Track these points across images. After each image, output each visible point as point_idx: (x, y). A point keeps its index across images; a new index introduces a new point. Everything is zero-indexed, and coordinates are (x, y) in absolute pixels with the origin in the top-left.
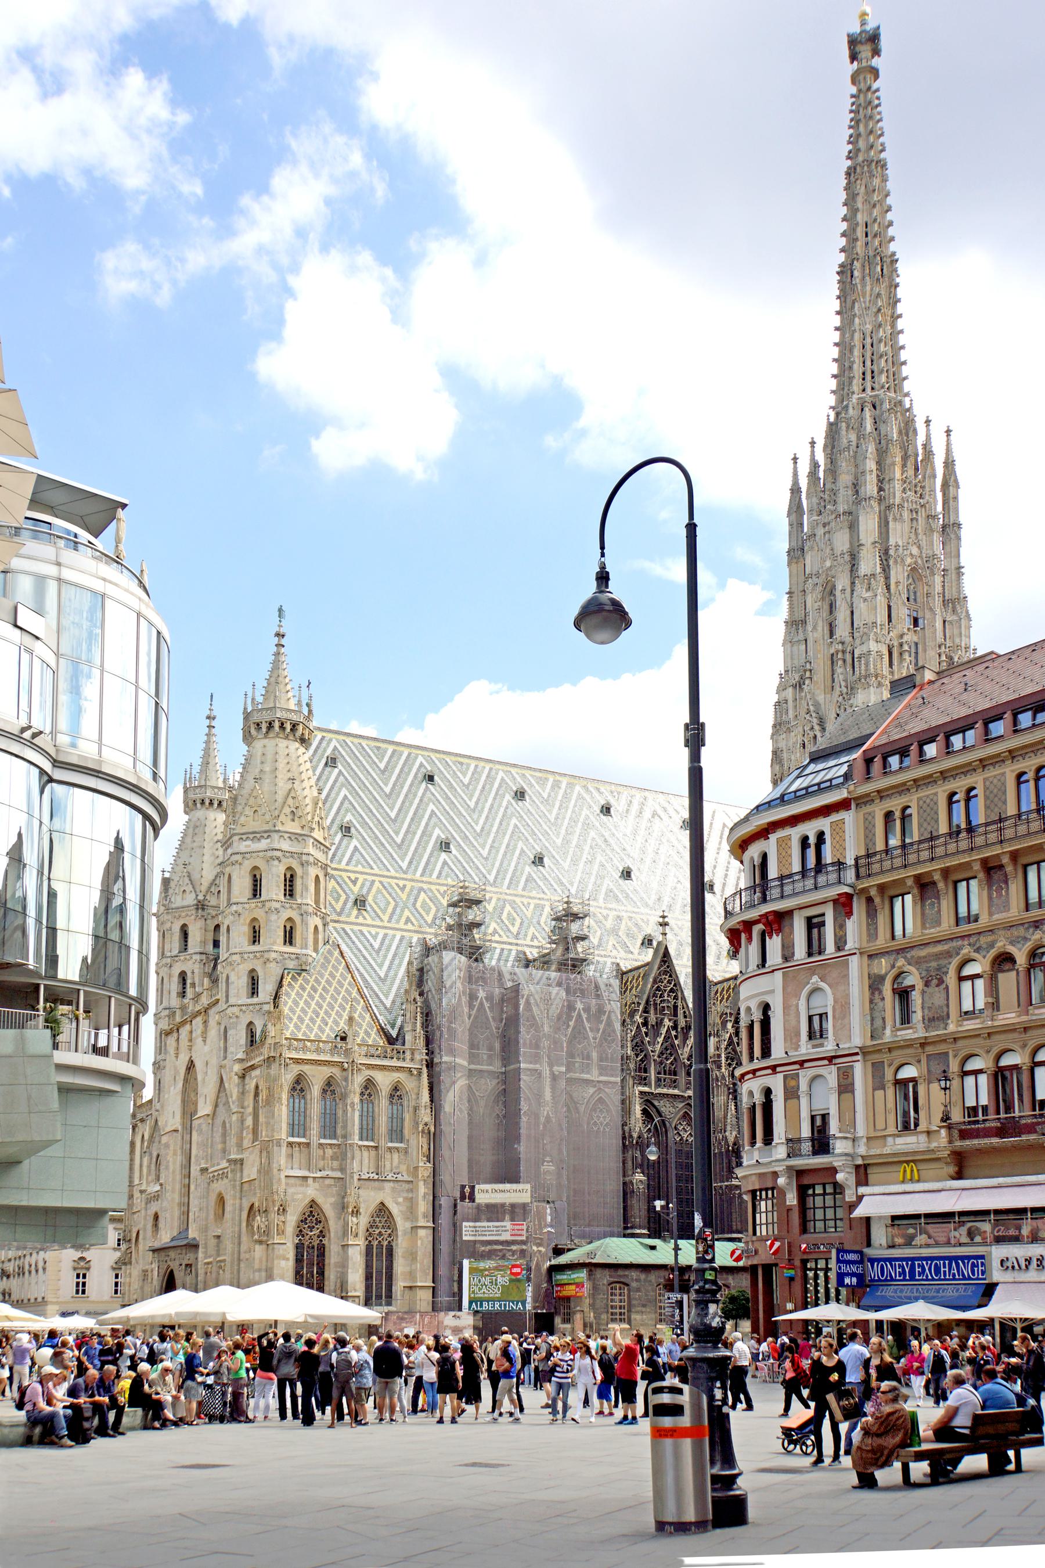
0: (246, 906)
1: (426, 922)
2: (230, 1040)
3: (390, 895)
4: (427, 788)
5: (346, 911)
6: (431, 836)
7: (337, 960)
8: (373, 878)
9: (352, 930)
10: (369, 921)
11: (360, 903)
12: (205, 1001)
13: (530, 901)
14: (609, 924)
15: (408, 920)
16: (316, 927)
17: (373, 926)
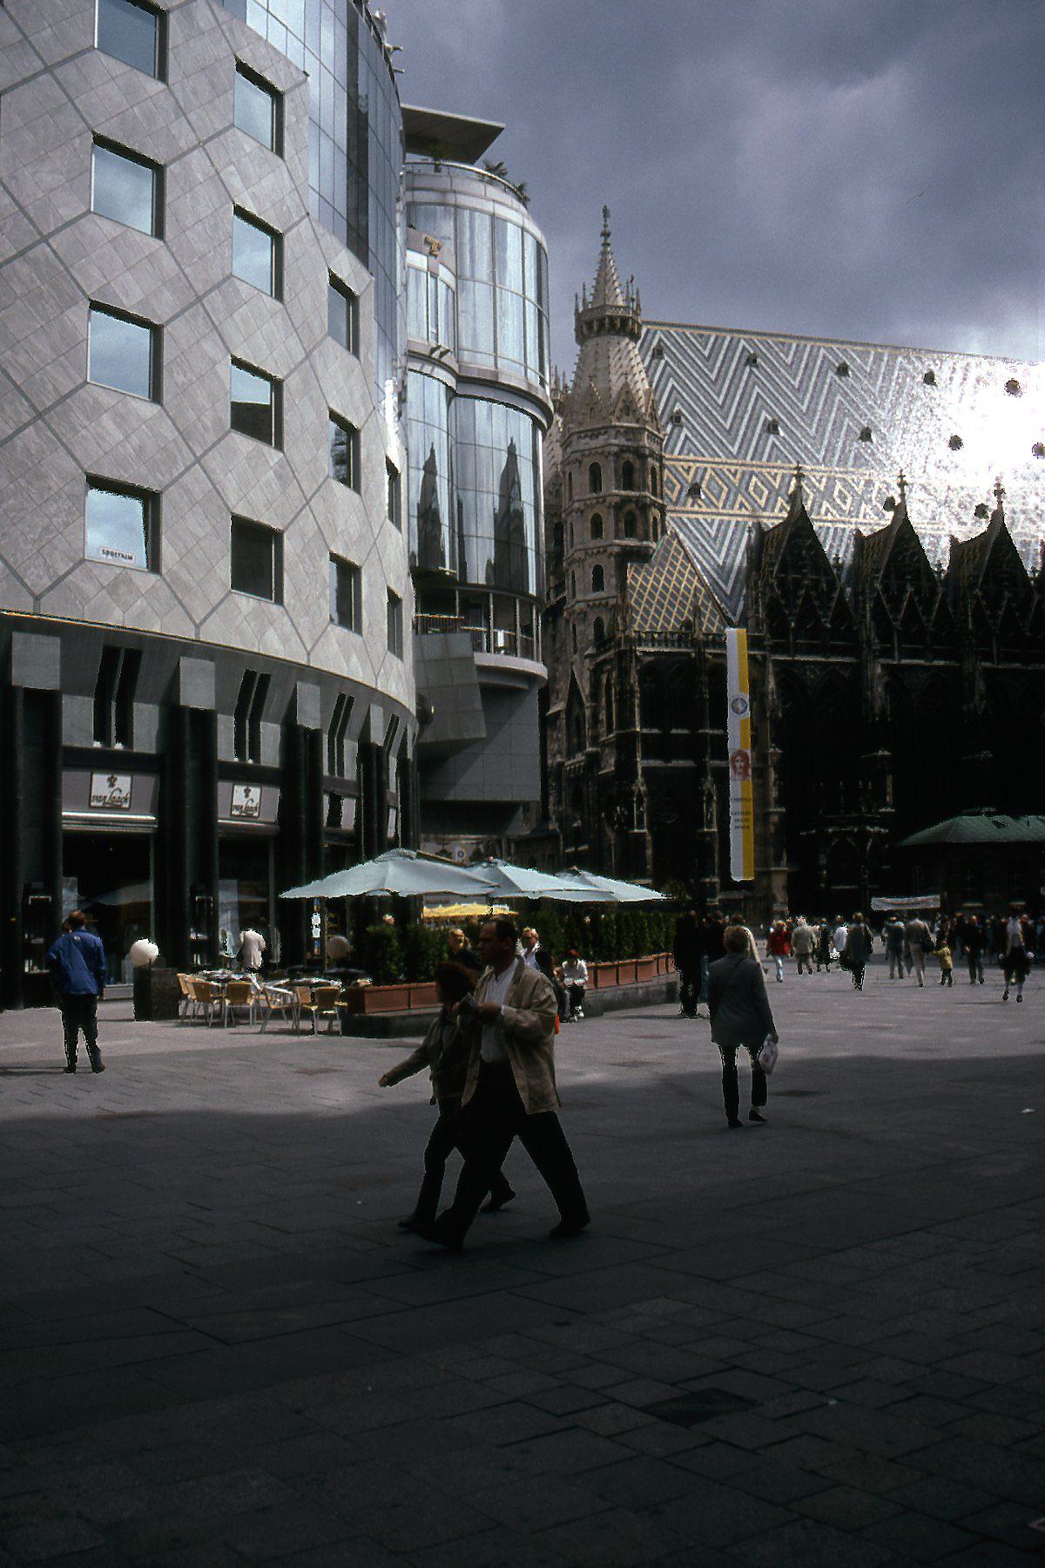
1: (759, 506)
4: (751, 372)
5: (682, 500)
6: (758, 419)
7: (676, 549)
9: (688, 519)
10: (704, 509)
11: (695, 491)
15: (742, 505)
16: (655, 518)
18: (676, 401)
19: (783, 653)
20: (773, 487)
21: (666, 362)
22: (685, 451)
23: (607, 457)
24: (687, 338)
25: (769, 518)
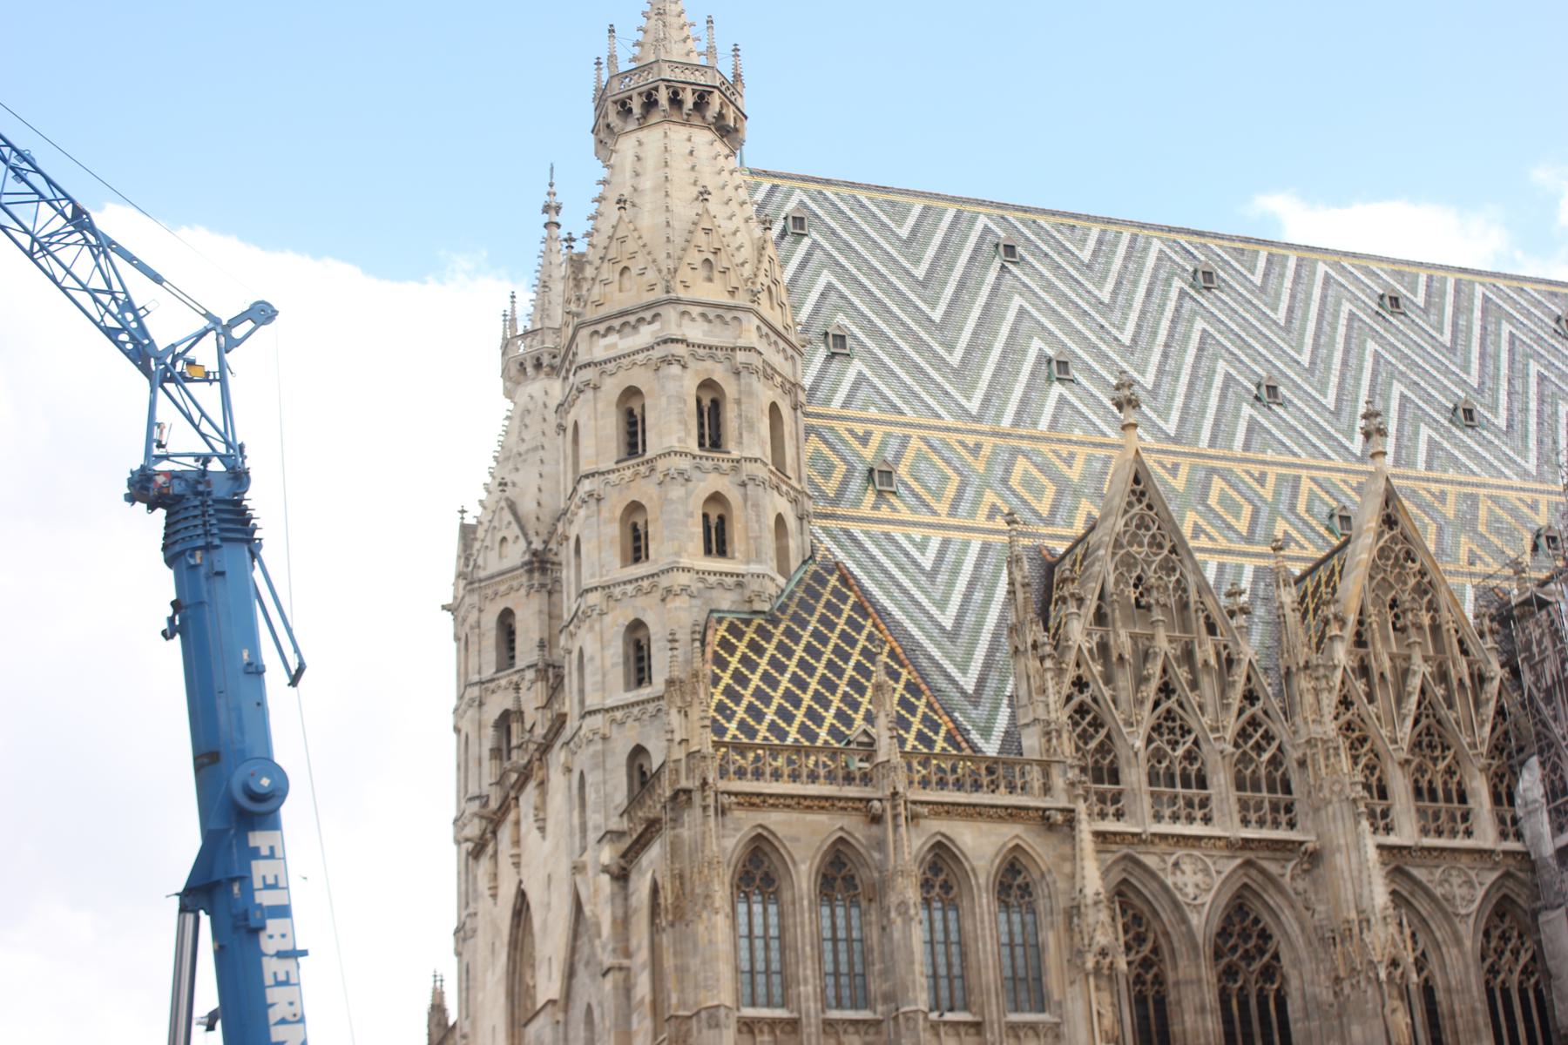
0: (613, 477)
1: (1035, 512)
2: (591, 796)
3: (948, 462)
5: (850, 495)
6: (1024, 352)
7: (835, 592)
8: (907, 431)
9: (866, 533)
10: (906, 515)
11: (880, 478)
12: (540, 731)
13: (1266, 468)
14: (1450, 510)
15: (993, 512)
16: (780, 520)
17: (915, 524)
18: (838, 308)
19: (1119, 815)
20: (1069, 480)
21: (815, 244)
22: (858, 402)
23: (657, 369)
24: (862, 206)
25: (1062, 538)
